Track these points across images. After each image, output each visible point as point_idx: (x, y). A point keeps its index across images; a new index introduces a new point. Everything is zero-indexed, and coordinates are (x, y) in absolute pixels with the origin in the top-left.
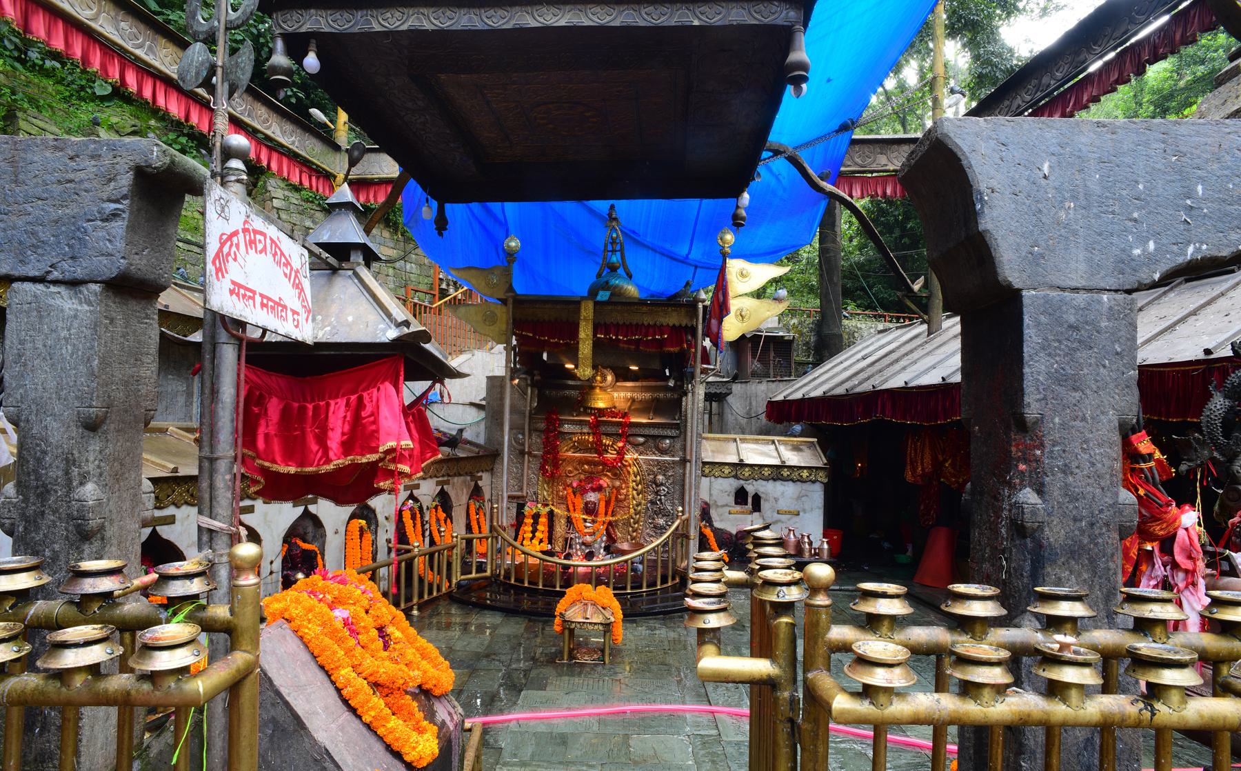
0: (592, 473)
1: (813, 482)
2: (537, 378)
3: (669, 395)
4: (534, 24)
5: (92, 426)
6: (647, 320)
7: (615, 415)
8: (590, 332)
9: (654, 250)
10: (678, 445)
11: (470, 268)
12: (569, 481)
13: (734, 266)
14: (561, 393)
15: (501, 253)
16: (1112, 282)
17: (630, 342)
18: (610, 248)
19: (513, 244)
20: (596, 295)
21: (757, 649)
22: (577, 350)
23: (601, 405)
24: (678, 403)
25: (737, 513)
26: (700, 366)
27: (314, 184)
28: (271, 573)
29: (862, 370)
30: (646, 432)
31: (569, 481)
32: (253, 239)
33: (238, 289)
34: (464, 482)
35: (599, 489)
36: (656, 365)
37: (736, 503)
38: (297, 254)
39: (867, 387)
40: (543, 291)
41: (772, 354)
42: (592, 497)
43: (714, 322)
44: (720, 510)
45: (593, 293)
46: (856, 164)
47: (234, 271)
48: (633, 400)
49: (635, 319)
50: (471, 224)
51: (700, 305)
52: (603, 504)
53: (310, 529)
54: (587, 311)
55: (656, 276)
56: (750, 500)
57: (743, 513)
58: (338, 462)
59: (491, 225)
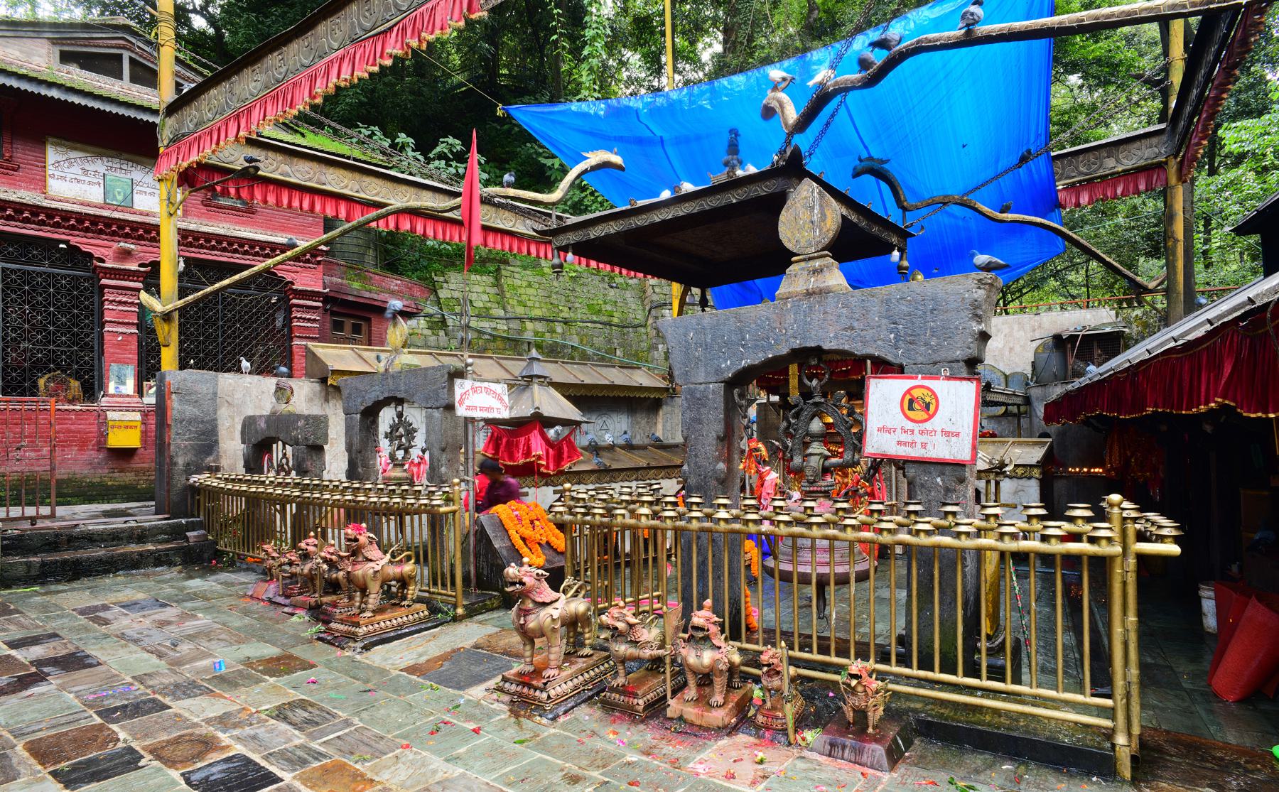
4: (657, 220)
5: (443, 450)
16: (714, 379)
32: (474, 390)
33: (468, 408)
38: (501, 388)
46: (1081, 174)
47: (467, 402)
58: (521, 462)
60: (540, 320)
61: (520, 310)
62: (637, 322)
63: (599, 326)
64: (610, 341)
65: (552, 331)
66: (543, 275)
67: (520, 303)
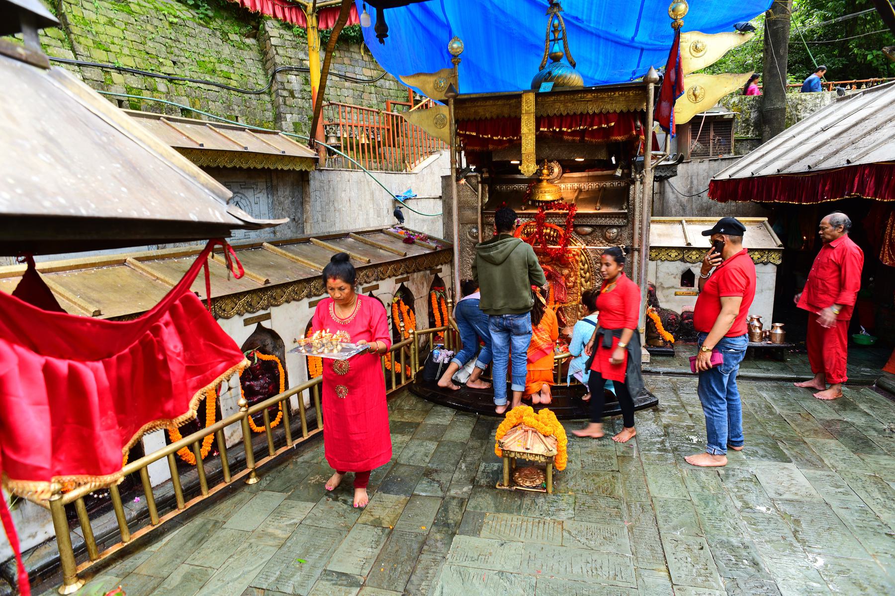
1: (765, 264)
2: (486, 175)
3: (616, 184)
6: (592, 109)
7: (561, 207)
8: (532, 126)
9: (599, 36)
10: (625, 234)
11: (419, 74)
13: (687, 39)
14: (511, 187)
15: (446, 55)
17: (574, 133)
18: (552, 37)
19: (455, 46)
20: (539, 87)
22: (519, 146)
23: (548, 197)
24: (626, 190)
25: (683, 294)
26: (651, 153)
27: (287, 14)
28: (230, 389)
29: (824, 144)
30: (593, 222)
34: (424, 276)
36: (602, 156)
37: (683, 284)
39: (838, 162)
40: (488, 89)
41: (712, 134)
43: (665, 105)
44: (666, 292)
45: (536, 85)
48: (580, 191)
49: (580, 108)
50: (414, 29)
51: (652, 86)
53: (269, 341)
54: (529, 104)
55: (601, 63)
56: (696, 282)
57: (689, 294)
59: (433, 28)
60: (133, 72)
61: (100, 56)
62: (259, 88)
63: (216, 89)
64: (229, 108)
65: (154, 90)
66: (131, 13)
67: (98, 45)
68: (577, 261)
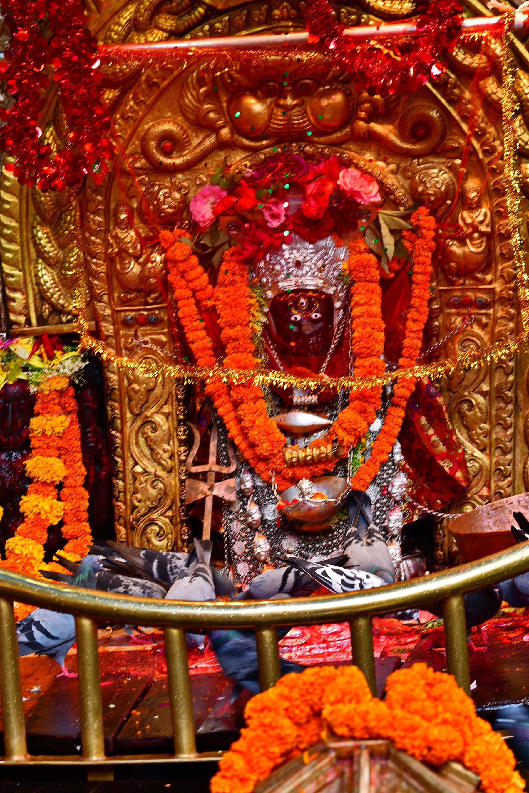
0: (288, 135)
12: (168, 198)
21: (408, 133)
31: (168, 198)
35: (341, 218)
42: (306, 266)
52: (369, 303)
68: (493, 109)
